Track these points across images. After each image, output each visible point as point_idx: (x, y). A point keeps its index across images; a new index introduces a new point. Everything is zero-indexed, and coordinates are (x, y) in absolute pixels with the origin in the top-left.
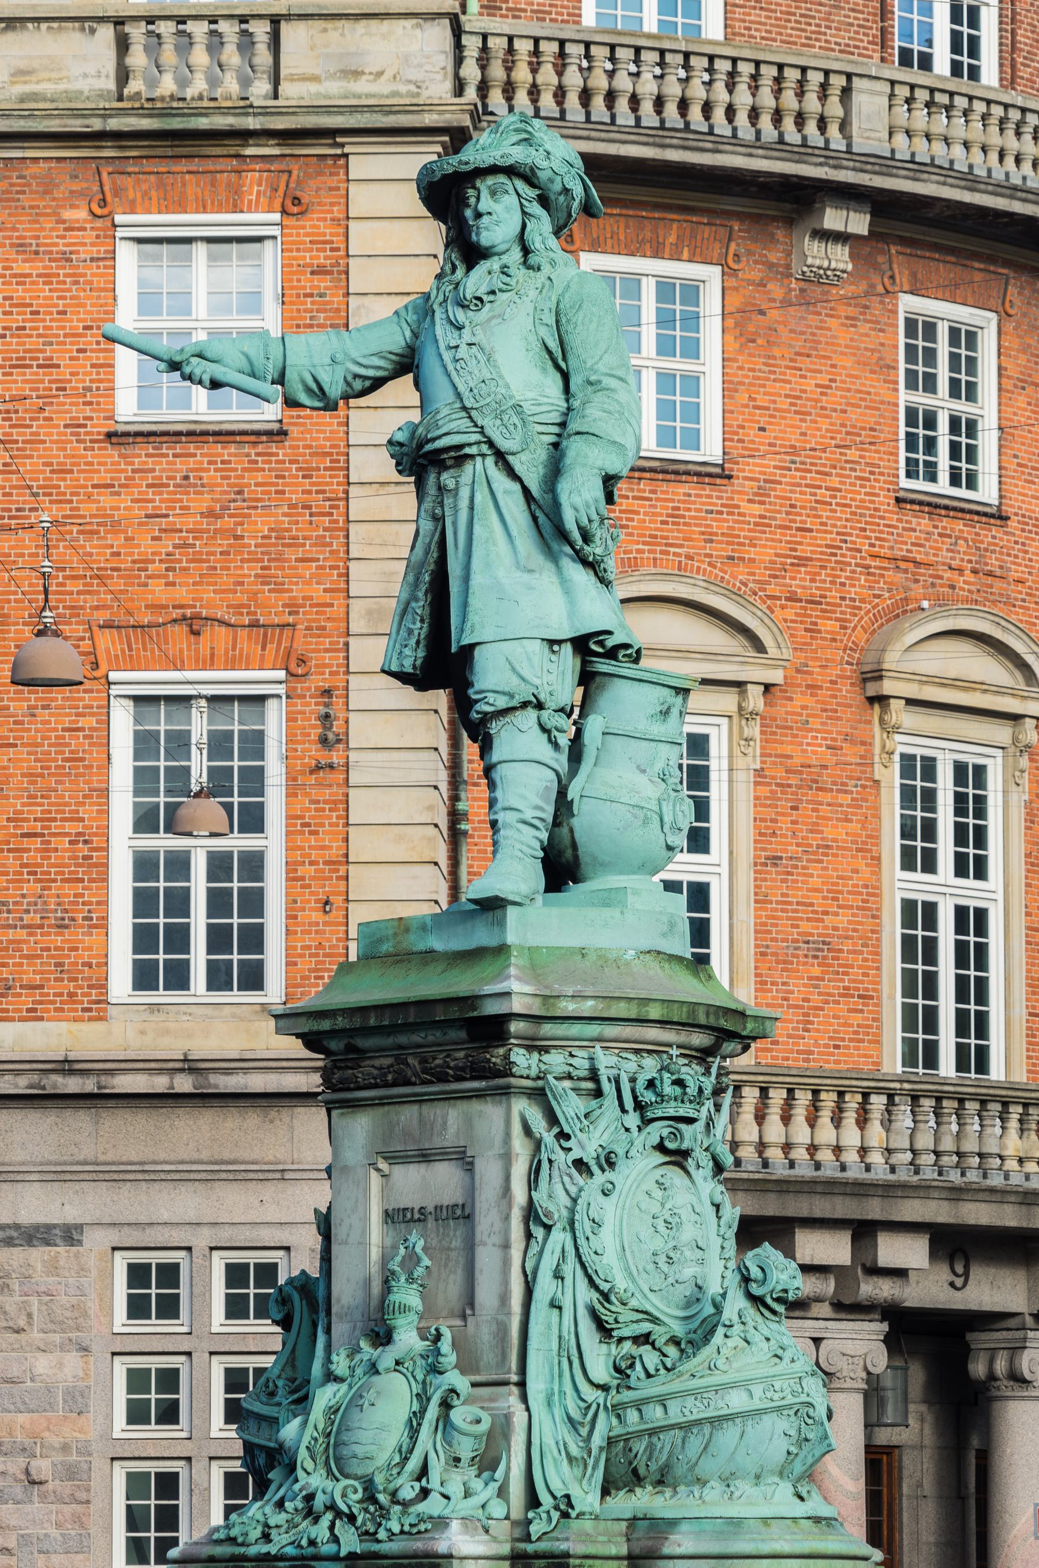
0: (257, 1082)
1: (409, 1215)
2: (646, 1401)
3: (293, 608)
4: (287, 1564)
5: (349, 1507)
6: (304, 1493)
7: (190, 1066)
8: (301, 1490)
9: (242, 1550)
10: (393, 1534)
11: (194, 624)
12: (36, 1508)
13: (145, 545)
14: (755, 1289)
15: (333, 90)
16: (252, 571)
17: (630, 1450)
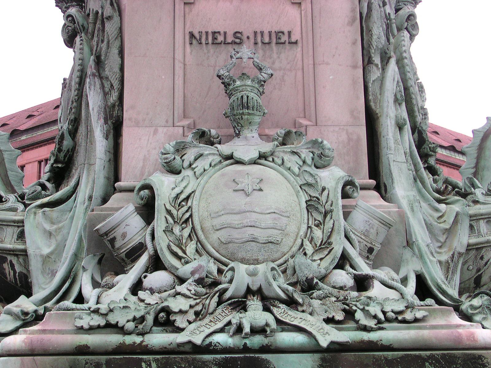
1: (220, 38)
4: (218, 356)
6: (197, 276)
8: (193, 273)
9: (138, 339)
10: (379, 322)
17: (482, 258)
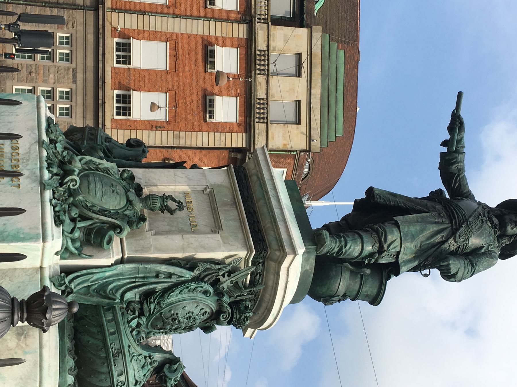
0: (100, 114)
2: (117, 324)
3: (178, 122)
5: (67, 183)
7: (104, 103)
11: (176, 106)
12: (25, 73)
13: (188, 99)
14: (167, 366)
15: (257, 131)
16: (184, 116)
